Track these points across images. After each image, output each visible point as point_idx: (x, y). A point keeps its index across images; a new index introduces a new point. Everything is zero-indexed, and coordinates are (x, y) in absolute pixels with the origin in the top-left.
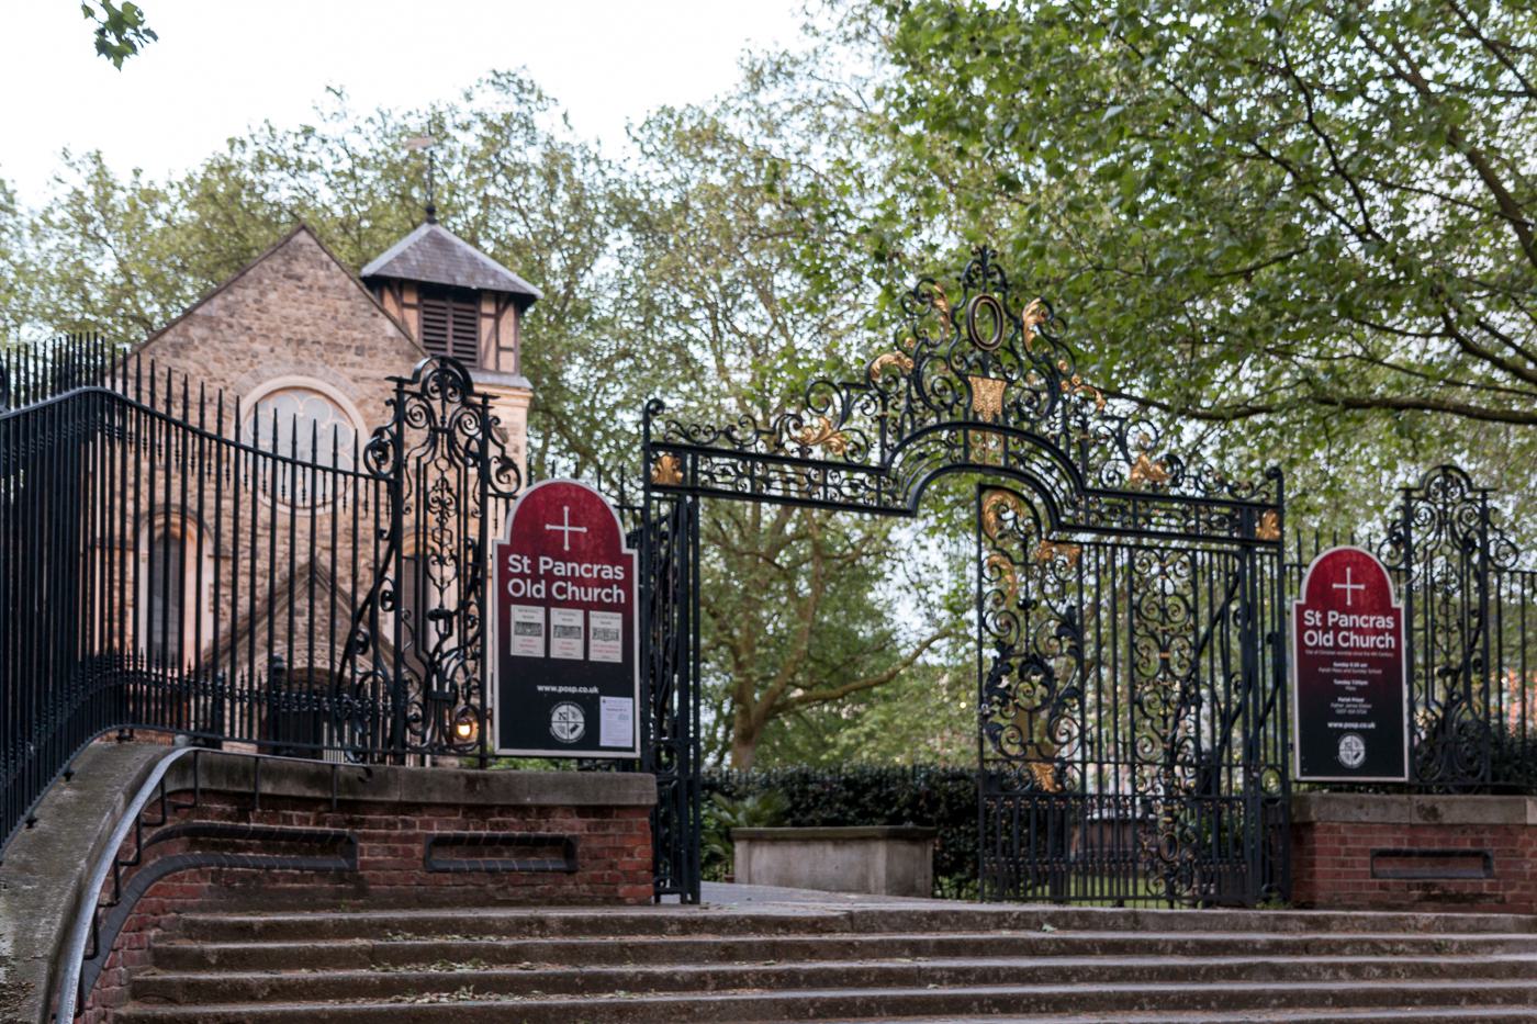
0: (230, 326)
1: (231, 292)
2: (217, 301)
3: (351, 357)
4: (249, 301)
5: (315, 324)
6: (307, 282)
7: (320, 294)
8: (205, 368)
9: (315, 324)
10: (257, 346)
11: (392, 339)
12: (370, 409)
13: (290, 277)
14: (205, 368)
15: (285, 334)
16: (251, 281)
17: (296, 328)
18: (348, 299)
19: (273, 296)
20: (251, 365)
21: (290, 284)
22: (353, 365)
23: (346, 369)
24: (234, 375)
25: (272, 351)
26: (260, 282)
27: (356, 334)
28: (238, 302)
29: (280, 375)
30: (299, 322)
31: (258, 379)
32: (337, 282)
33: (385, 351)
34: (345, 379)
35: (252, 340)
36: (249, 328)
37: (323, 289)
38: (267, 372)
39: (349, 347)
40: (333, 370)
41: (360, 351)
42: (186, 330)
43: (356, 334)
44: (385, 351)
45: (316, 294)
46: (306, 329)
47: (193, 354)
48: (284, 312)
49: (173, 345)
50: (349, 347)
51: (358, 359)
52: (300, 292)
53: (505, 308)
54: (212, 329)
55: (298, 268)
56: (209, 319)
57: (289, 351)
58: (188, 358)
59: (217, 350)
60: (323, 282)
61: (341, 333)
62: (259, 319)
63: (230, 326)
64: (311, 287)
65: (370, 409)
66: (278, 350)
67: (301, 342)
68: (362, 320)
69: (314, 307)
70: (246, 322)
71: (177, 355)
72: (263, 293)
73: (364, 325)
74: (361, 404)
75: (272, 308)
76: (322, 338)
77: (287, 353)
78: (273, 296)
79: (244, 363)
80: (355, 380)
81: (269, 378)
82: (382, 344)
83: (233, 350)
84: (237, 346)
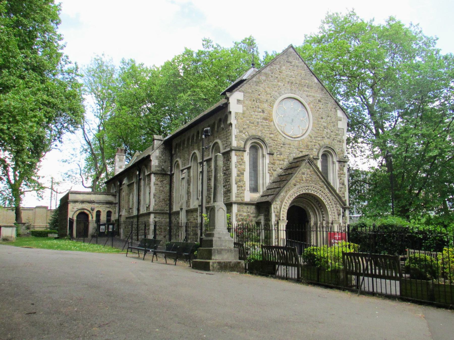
0: (272, 77)
1: (272, 66)
2: (268, 68)
3: (306, 89)
4: (277, 69)
5: (295, 77)
6: (293, 64)
7: (296, 68)
8: (265, 90)
9: (295, 77)
10: (279, 83)
11: (317, 83)
12: (312, 106)
13: (288, 62)
14: (265, 90)
15: (287, 80)
16: (277, 62)
17: (291, 78)
18: (304, 70)
19: (284, 68)
20: (278, 90)
21: (289, 64)
22: (306, 91)
23: (305, 93)
24: (273, 92)
25: (284, 85)
26: (280, 63)
27: (307, 81)
28: (274, 69)
29: (286, 93)
30: (291, 77)
31: (280, 94)
32: (301, 64)
33: (315, 87)
34: (304, 96)
35: (278, 81)
36: (277, 78)
37: (297, 66)
38: (283, 92)
39: (305, 85)
40: (301, 92)
42: (259, 77)
43: (307, 81)
45: (296, 68)
46: (293, 79)
47: (261, 85)
48: (287, 73)
49: (255, 82)
50: (305, 85)
51: (308, 89)
52: (291, 67)
54: (267, 77)
55: (290, 60)
56: (266, 74)
57: (289, 86)
58: (260, 86)
59: (269, 84)
60: (297, 64)
61: (303, 81)
62: (280, 75)
64: (294, 66)
66: (286, 85)
67: (292, 83)
68: (308, 77)
69: (295, 72)
70: (276, 76)
71: (257, 85)
72: (281, 67)
73: (309, 79)
74: (309, 104)
75: (283, 71)
76: (298, 82)
77: (288, 86)
78: (284, 68)
79: (276, 89)
80: (307, 96)
81: (283, 94)
82: (314, 85)
83: (273, 85)
84: (274, 83)
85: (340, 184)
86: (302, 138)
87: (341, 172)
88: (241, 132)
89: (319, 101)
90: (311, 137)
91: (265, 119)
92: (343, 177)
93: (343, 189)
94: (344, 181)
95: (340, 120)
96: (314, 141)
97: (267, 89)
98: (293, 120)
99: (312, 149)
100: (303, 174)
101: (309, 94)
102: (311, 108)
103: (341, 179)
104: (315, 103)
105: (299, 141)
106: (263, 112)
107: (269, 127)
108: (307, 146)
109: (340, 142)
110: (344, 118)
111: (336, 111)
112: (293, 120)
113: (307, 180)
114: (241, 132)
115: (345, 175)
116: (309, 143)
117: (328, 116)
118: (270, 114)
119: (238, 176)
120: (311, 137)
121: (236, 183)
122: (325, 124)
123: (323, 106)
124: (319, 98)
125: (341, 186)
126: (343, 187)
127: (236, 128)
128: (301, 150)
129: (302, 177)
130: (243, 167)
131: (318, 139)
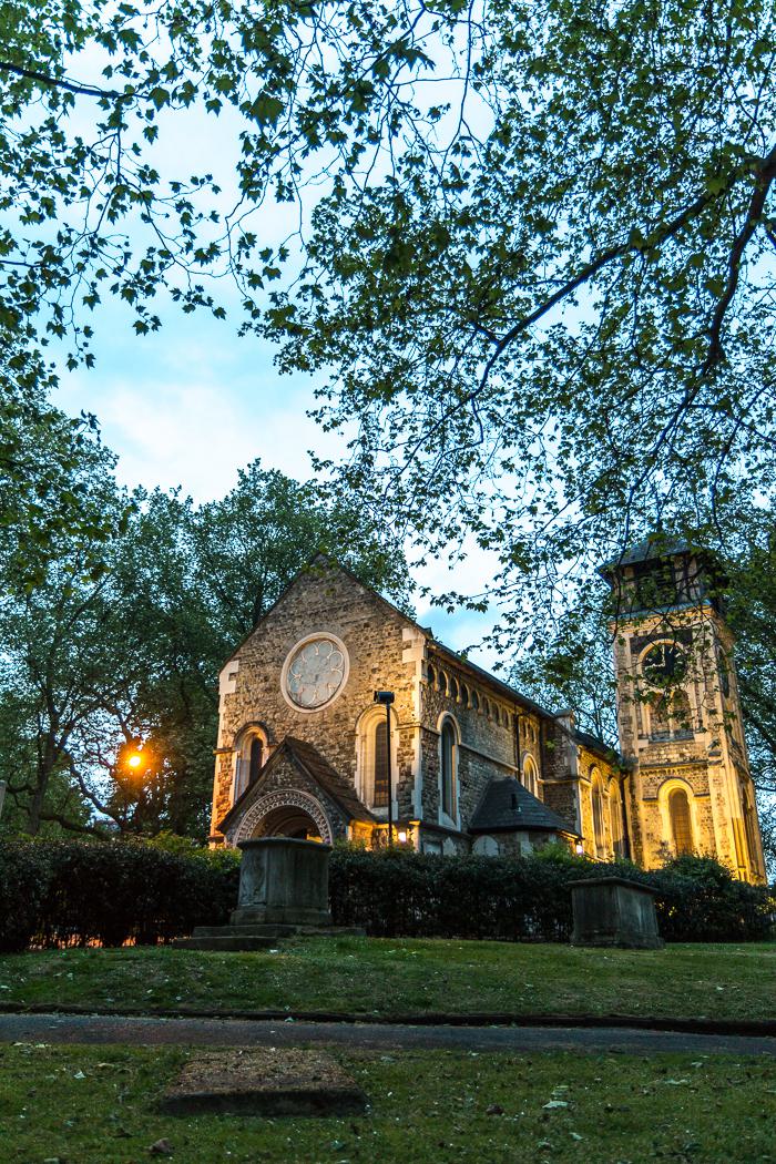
27: (345, 600)
31: (295, 640)
41: (346, 609)
43: (345, 600)
44: (359, 604)
47: (267, 637)
53: (689, 564)
63: (284, 616)
65: (350, 640)
71: (260, 640)
74: (345, 639)
84: (286, 627)
85: (401, 774)
86: (328, 704)
87: (406, 749)
88: (231, 722)
89: (367, 625)
90: (345, 698)
91: (268, 690)
92: (409, 759)
93: (407, 786)
94: (410, 767)
95: (409, 647)
96: (352, 703)
97: (276, 641)
98: (317, 677)
99: (346, 719)
100: (279, 772)
101: (345, 620)
102: (350, 647)
103: (403, 765)
104: (356, 632)
105: (323, 711)
106: (266, 679)
107: (274, 702)
108: (337, 716)
109: (405, 689)
110: (416, 640)
111: (401, 632)
112: (317, 677)
113: (283, 783)
114: (231, 722)
115: (413, 754)
116: (341, 711)
117: (382, 648)
118: (277, 680)
119: (221, 793)
120: (345, 698)
121: (218, 806)
122: (376, 666)
123: (373, 634)
124: (366, 621)
125: (404, 778)
126: (409, 780)
127: (224, 718)
128: (324, 726)
129: (276, 779)
130: (228, 779)
131: (359, 697)
